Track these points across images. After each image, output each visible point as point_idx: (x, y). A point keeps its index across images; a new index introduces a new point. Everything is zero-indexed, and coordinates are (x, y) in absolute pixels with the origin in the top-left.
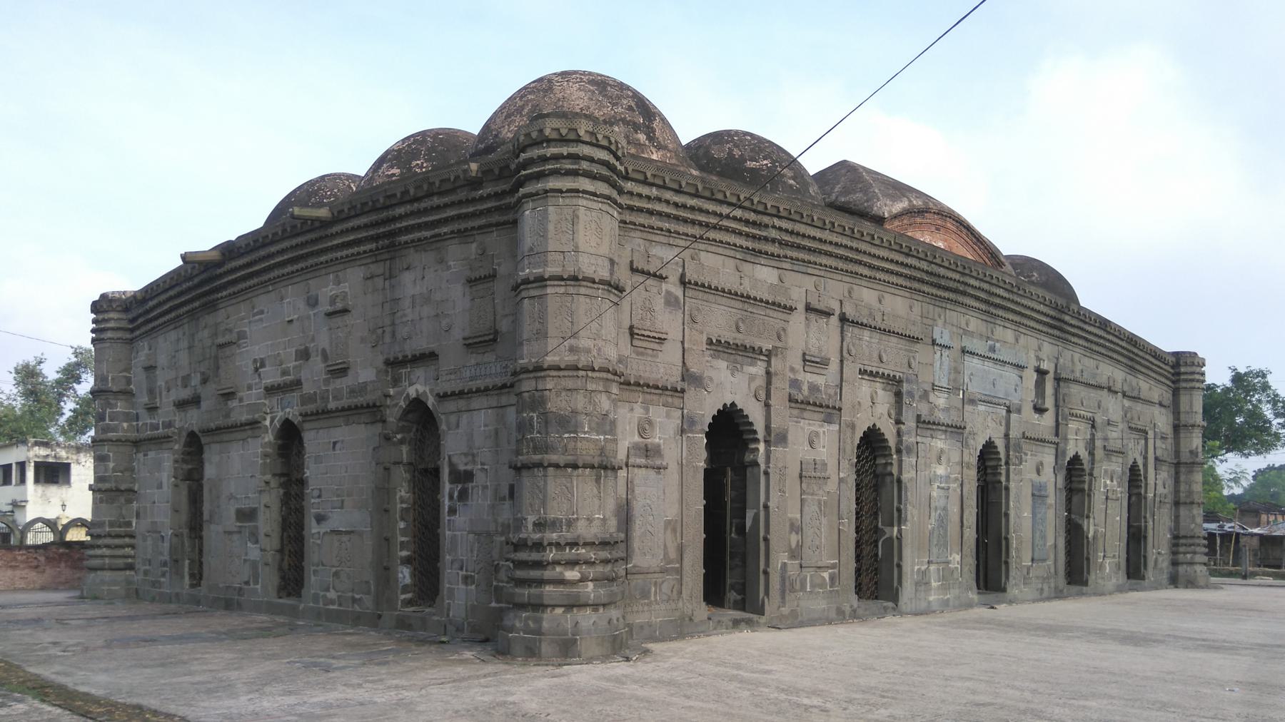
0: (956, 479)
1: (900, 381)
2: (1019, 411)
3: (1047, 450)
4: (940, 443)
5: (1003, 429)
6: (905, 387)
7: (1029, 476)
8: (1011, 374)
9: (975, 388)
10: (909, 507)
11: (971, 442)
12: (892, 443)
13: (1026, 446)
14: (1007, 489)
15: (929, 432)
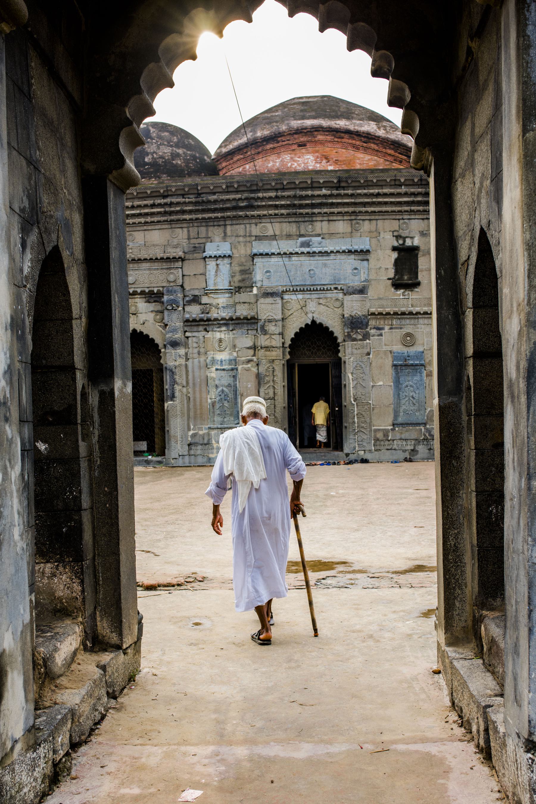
0: (249, 361)
1: (160, 295)
2: (362, 291)
3: (421, 321)
4: (219, 334)
5: (339, 311)
6: (165, 298)
7: (385, 348)
8: (351, 261)
9: (276, 283)
10: (177, 388)
11: (271, 328)
12: (158, 340)
13: (372, 323)
14: (345, 362)
15: (201, 328)
